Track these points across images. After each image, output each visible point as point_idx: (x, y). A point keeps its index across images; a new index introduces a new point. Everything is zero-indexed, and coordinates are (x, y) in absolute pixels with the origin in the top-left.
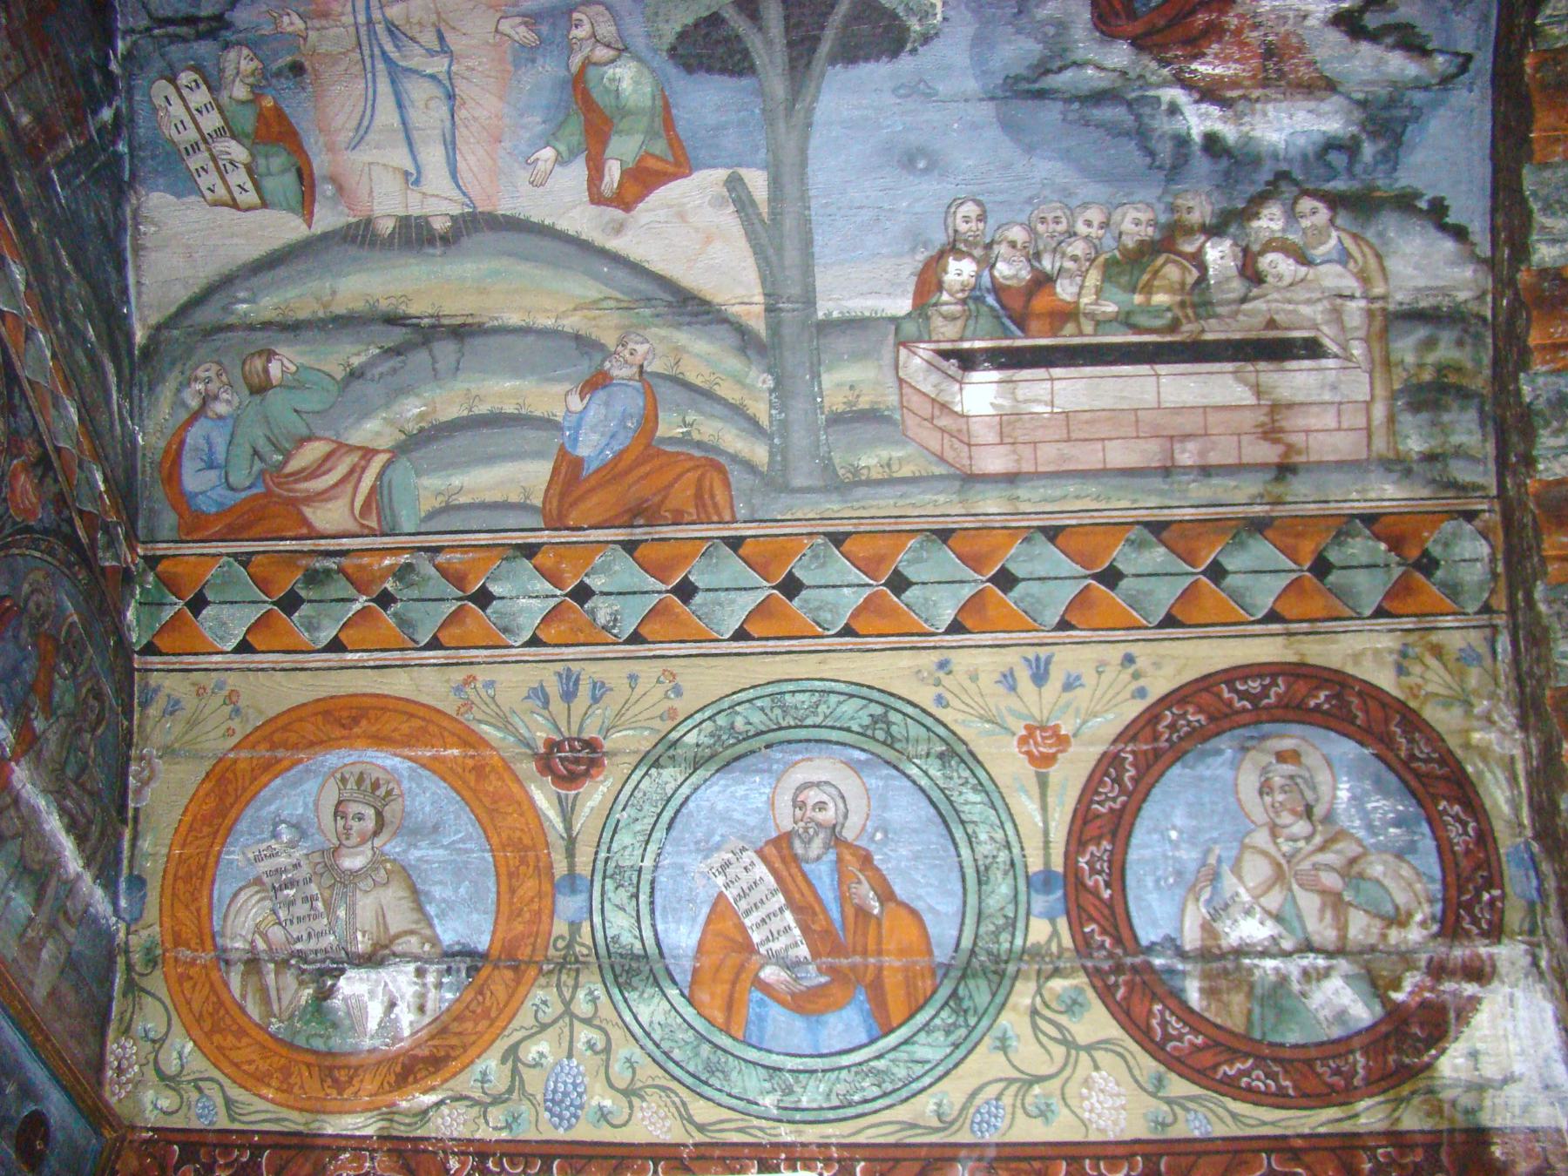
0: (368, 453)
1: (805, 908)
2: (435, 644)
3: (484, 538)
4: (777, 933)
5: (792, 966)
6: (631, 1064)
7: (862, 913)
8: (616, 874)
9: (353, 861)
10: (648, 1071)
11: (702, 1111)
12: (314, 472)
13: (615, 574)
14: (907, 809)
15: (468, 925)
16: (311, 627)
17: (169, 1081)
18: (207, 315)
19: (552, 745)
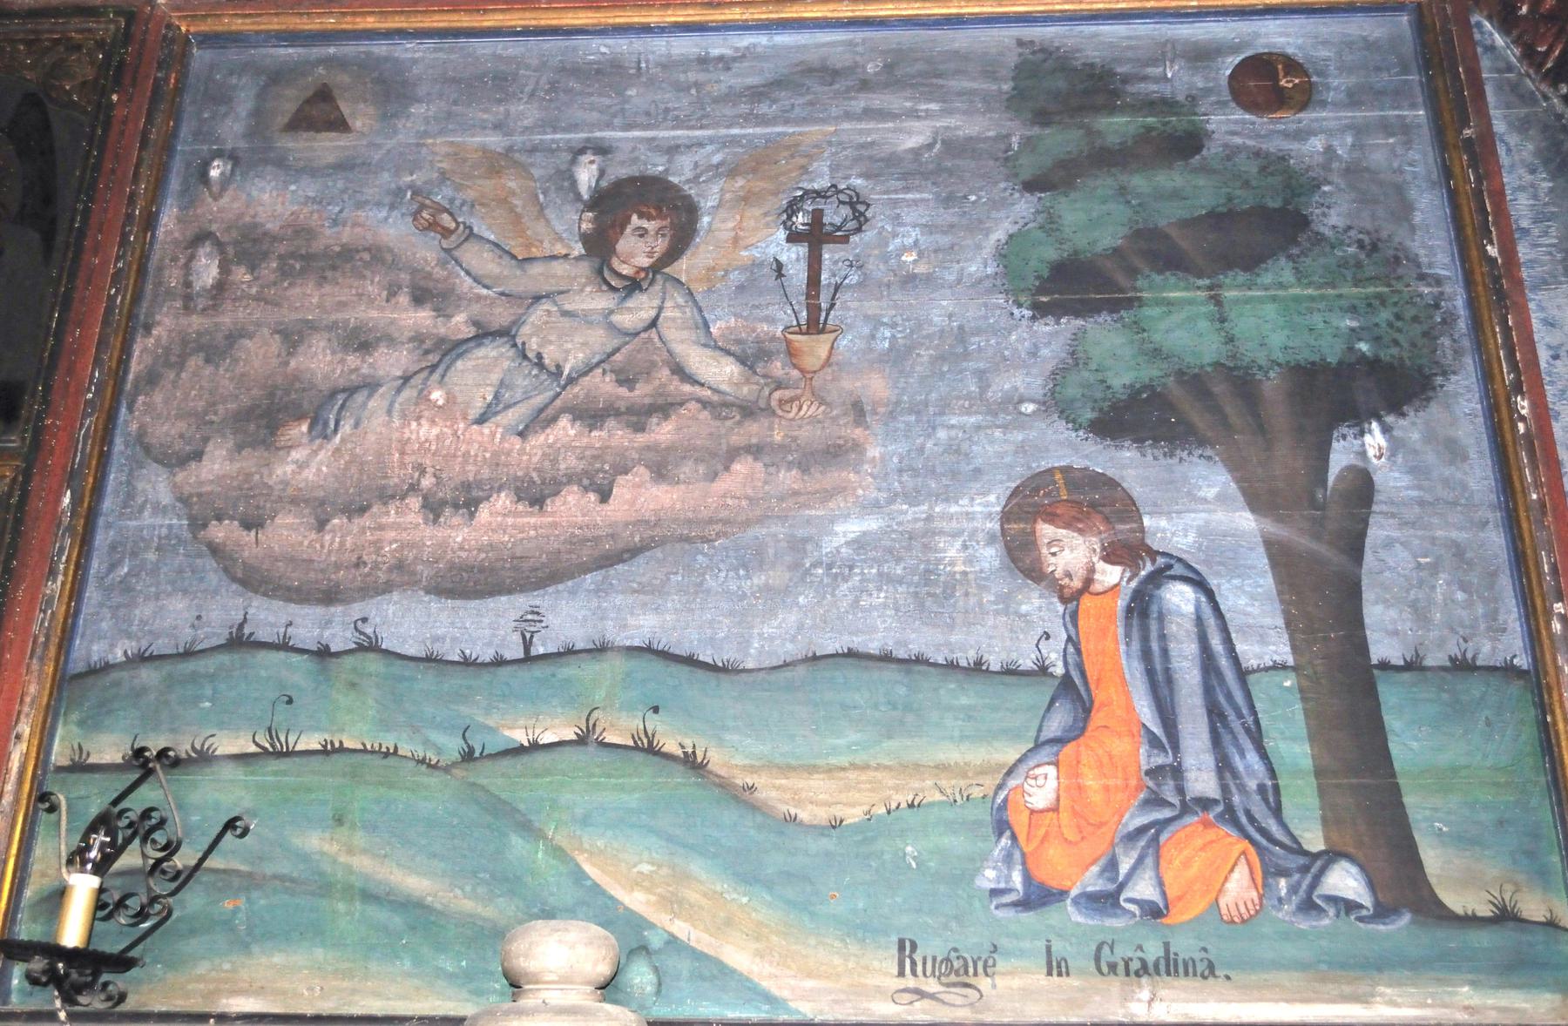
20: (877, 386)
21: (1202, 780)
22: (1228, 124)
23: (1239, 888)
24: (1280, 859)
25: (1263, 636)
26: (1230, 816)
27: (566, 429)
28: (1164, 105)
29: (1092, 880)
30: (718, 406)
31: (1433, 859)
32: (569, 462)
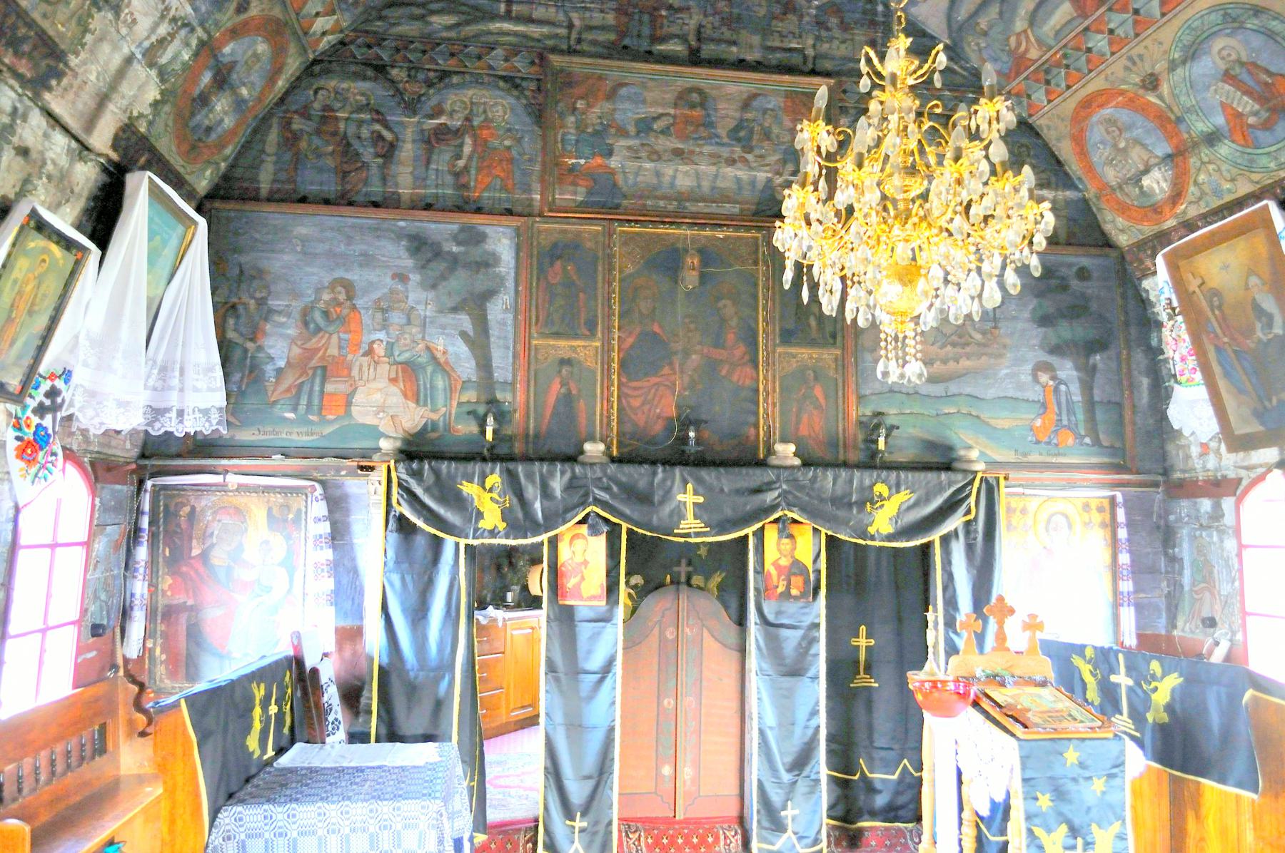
0: (1025, 31)
1: (1248, 92)
2: (1090, 71)
3: (1073, 34)
4: (1246, 105)
5: (1256, 114)
6: (1229, 171)
7: (1266, 84)
8: (1188, 110)
9: (1122, 145)
10: (1235, 171)
11: (1255, 177)
12: (1019, 44)
13: (1115, 20)
14: (1257, 41)
15: (1163, 148)
16: (1058, 85)
17: (1122, 231)
18: (955, 27)
19: (1143, 81)
20: (1008, 341)
21: (1065, 422)
22: (1075, 284)
23: (1070, 441)
24: (1079, 437)
25: (1077, 398)
26: (1069, 428)
27: (949, 348)
28: (1063, 278)
29: (1046, 439)
30: (979, 344)
31: (1101, 436)
32: (951, 355)
